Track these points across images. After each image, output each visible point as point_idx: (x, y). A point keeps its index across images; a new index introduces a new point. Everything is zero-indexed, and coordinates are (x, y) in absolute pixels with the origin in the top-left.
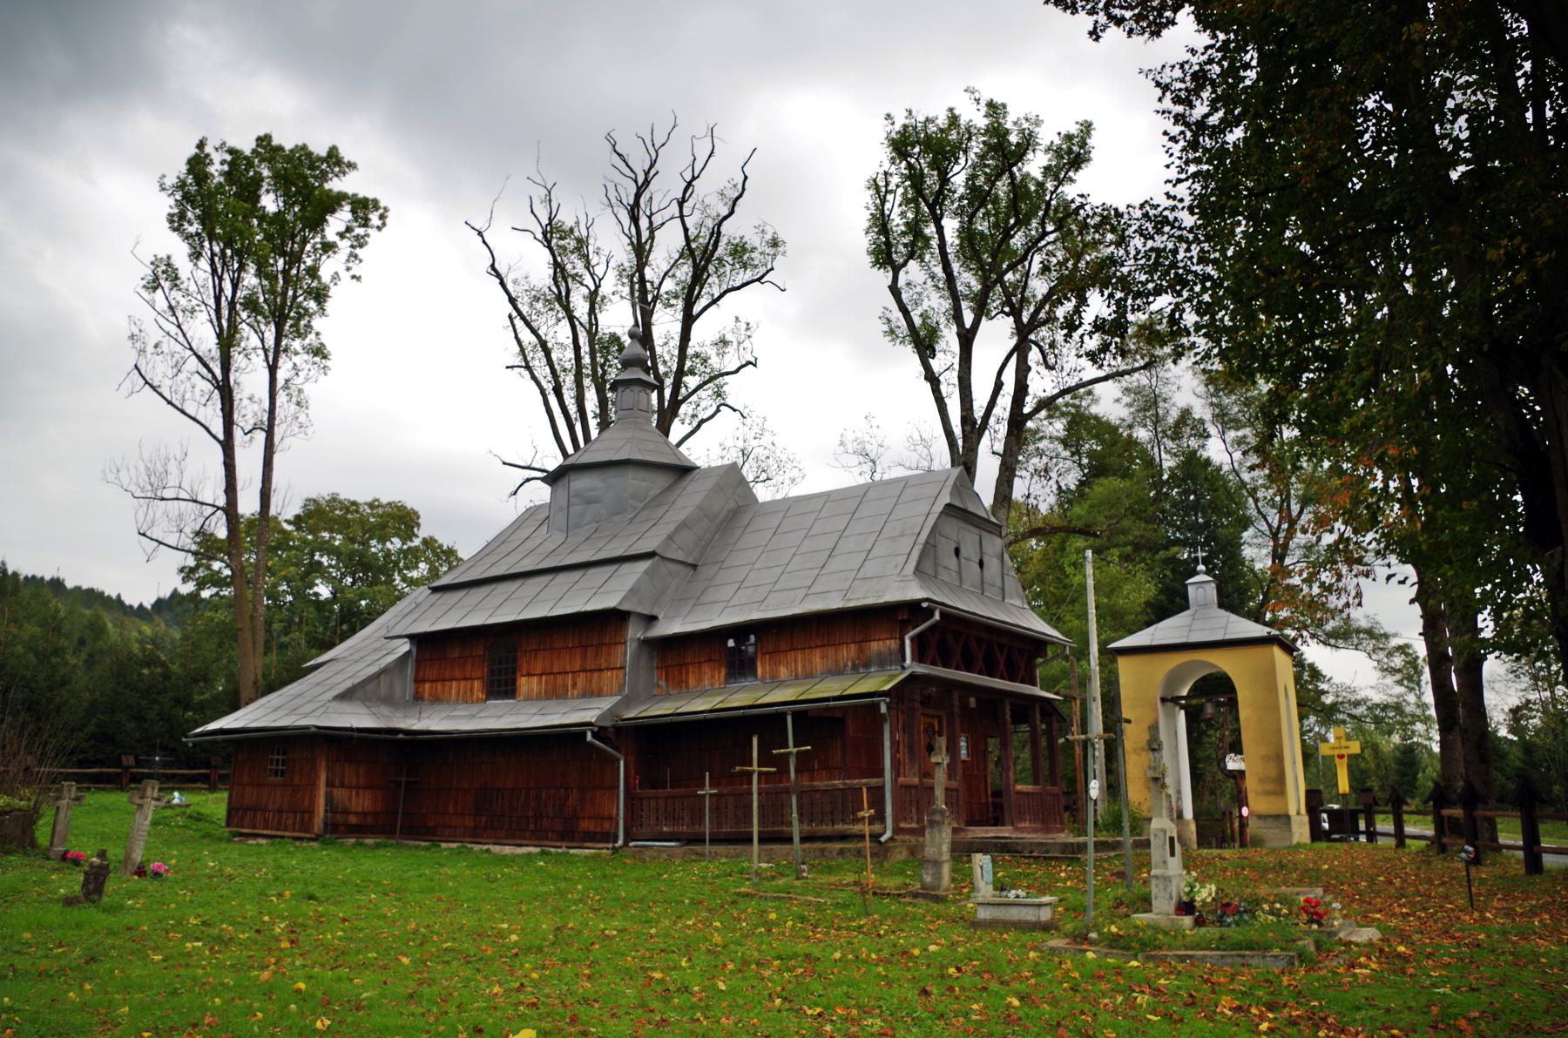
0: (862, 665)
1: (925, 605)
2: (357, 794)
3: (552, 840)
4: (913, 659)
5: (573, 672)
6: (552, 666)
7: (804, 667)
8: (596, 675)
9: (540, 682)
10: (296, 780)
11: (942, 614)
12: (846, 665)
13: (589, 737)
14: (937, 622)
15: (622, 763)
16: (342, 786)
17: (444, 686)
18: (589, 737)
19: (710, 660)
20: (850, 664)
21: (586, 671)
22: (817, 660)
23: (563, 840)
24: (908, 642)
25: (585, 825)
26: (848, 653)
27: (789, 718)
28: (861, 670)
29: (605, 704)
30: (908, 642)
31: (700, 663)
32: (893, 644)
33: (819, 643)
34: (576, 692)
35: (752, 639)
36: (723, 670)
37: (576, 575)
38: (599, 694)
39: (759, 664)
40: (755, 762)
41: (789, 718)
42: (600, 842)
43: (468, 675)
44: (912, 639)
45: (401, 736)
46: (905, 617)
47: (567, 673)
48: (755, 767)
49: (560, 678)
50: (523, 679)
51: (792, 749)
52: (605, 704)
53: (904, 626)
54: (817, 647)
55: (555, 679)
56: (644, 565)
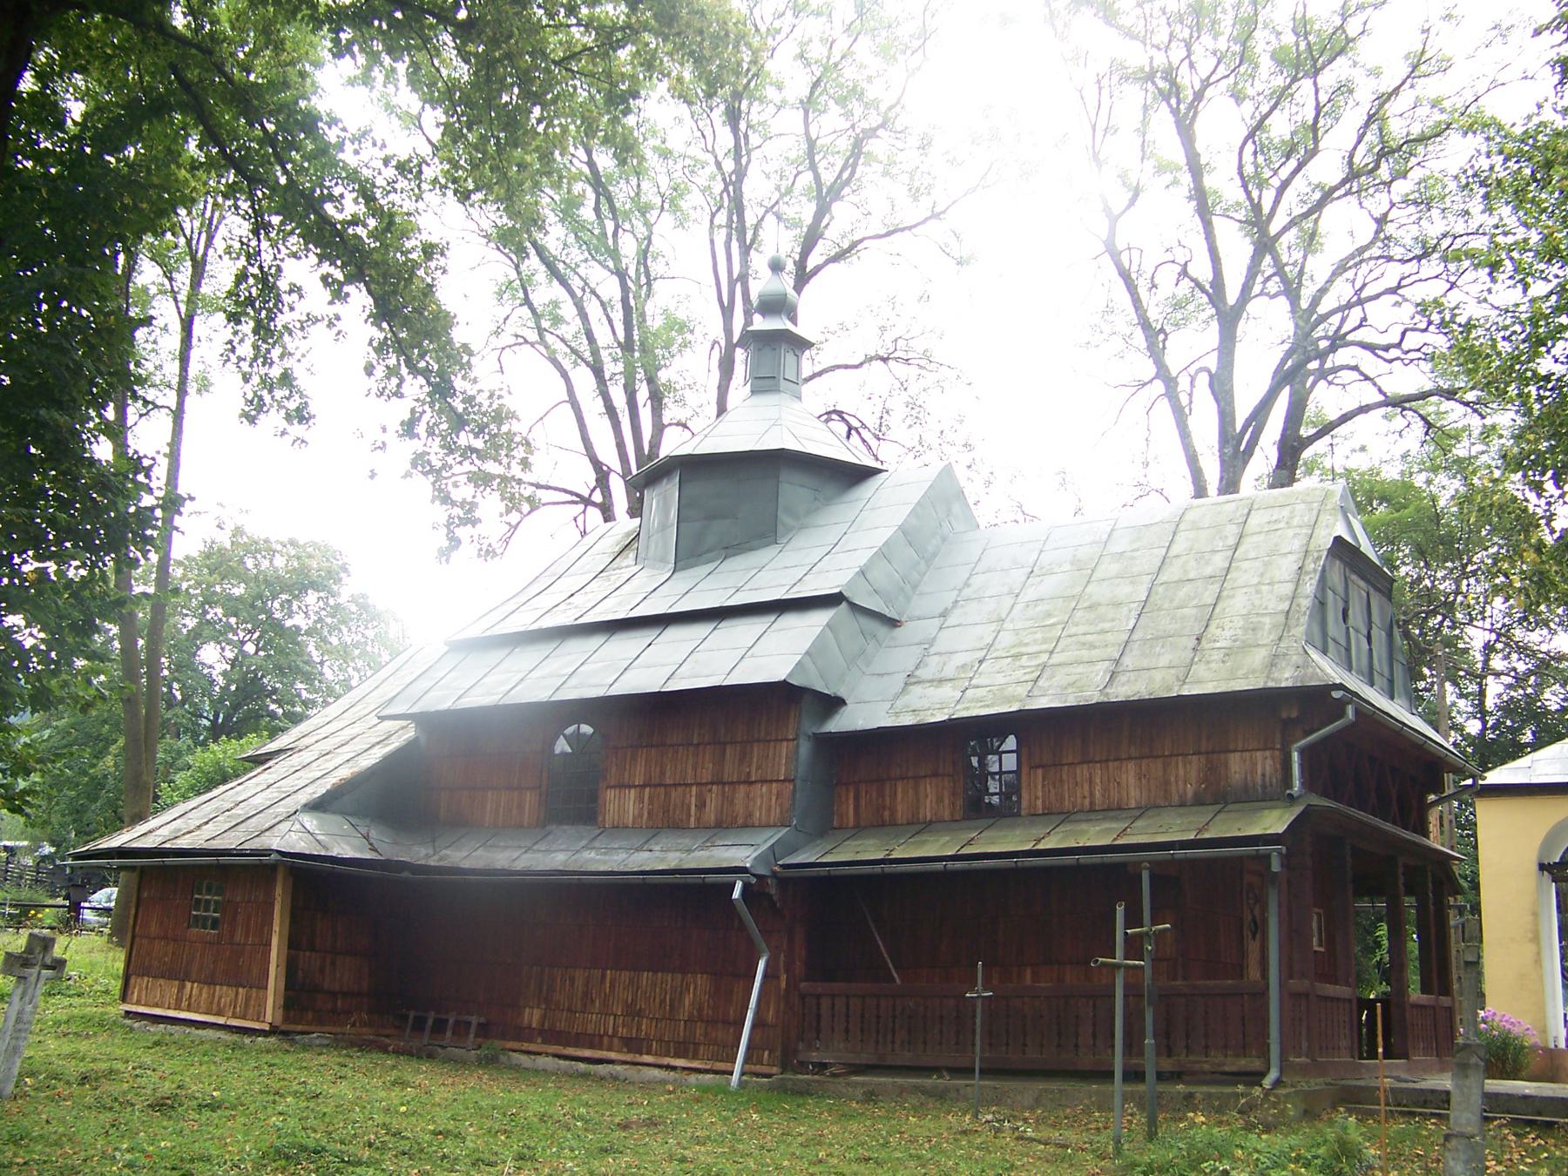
0: (1217, 796)
1: (1336, 694)
2: (333, 963)
4: (1303, 784)
5: (698, 784)
6: (663, 773)
7: (1105, 790)
8: (742, 789)
10: (239, 937)
11: (1357, 712)
13: (736, 894)
14: (1353, 725)
16: (313, 950)
18: (736, 894)
19: (935, 775)
22: (1130, 781)
24: (1295, 756)
26: (1187, 774)
27: (1145, 875)
29: (766, 840)
30: (1295, 756)
31: (917, 778)
33: (1134, 752)
35: (1011, 742)
37: (699, 630)
38: (748, 825)
40: (1119, 951)
41: (1145, 875)
44: (1302, 752)
45: (405, 874)
46: (1294, 714)
47: (691, 785)
48: (1119, 958)
49: (675, 794)
50: (611, 794)
52: (766, 840)
53: (1289, 730)
54: (1130, 758)
55: (667, 795)
56: (818, 620)
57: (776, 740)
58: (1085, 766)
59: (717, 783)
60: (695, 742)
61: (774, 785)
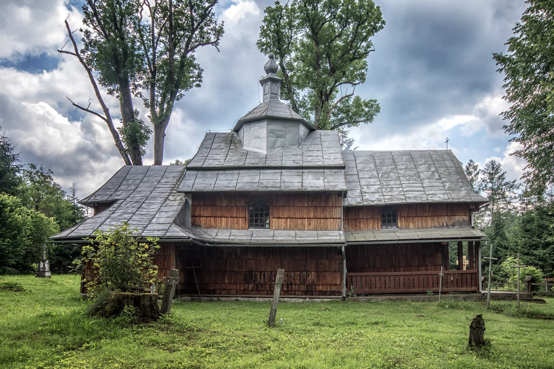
3: (298, 295)
8: (323, 221)
9: (286, 222)
12: (443, 224)
15: (345, 261)
17: (215, 221)
20: (445, 224)
21: (317, 218)
23: (306, 295)
25: (320, 288)
26: (444, 220)
28: (450, 227)
32: (466, 218)
33: (430, 214)
34: (311, 228)
36: (380, 222)
39: (399, 221)
42: (329, 295)
43: (235, 215)
47: (305, 218)
50: (274, 220)
51: (491, 258)
57: (335, 207)
58: (416, 218)
59: (315, 218)
60: (306, 206)
61: (335, 219)
